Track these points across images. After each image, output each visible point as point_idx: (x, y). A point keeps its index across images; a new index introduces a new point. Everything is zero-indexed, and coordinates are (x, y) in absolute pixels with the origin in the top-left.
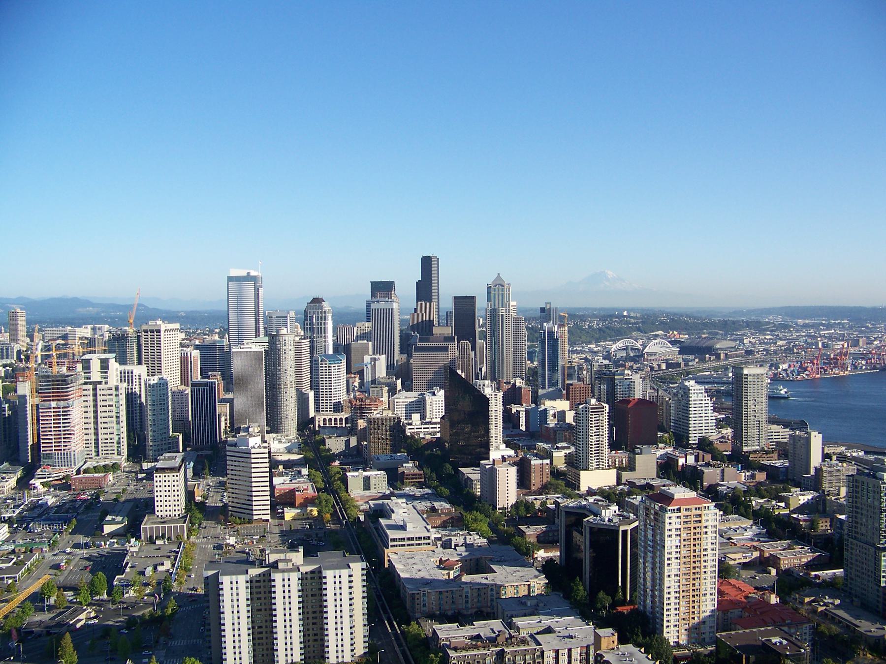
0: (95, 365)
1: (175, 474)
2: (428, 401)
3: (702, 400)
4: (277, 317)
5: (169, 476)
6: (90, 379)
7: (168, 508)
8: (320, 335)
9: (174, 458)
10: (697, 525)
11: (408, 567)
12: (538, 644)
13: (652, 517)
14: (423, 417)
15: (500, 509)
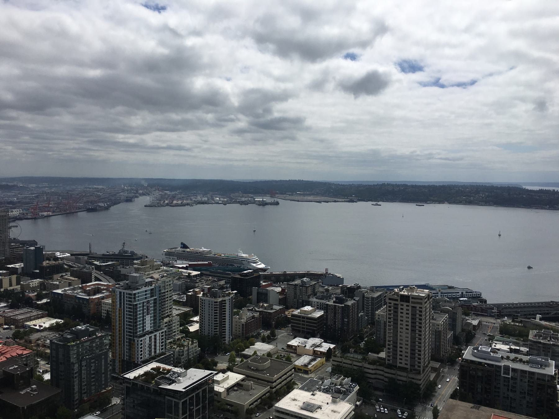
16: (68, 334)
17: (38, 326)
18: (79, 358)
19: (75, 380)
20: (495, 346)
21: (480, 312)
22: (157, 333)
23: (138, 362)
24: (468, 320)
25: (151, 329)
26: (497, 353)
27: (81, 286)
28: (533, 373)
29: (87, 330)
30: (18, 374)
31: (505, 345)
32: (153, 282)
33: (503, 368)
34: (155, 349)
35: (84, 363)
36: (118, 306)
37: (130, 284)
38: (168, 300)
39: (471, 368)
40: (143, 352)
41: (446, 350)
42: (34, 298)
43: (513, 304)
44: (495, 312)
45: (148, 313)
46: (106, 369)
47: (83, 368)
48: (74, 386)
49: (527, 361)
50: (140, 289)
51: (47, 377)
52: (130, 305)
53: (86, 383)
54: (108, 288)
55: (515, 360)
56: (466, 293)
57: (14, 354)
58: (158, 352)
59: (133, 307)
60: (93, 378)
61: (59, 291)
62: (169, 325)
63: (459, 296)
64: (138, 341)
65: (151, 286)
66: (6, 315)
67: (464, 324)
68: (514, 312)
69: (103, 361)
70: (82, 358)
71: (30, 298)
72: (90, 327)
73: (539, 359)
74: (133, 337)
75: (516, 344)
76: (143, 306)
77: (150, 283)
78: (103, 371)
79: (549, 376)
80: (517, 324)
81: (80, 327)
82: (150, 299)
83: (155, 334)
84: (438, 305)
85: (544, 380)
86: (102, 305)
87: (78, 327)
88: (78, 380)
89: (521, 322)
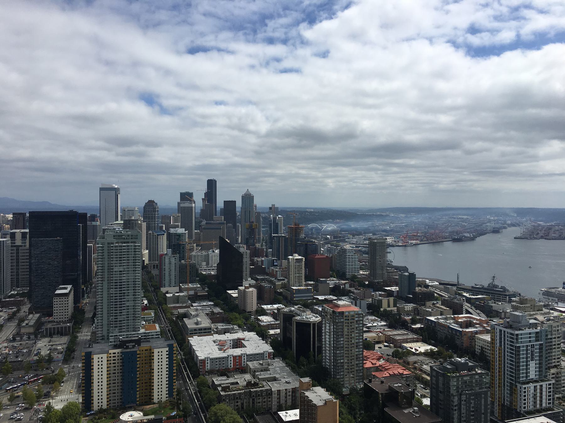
0: (18, 237)
1: (66, 297)
2: (210, 255)
3: (353, 255)
4: (128, 210)
5: (62, 298)
6: (15, 244)
7: (61, 317)
8: (152, 220)
9: (66, 288)
10: (352, 321)
11: (199, 345)
12: (270, 387)
13: (329, 317)
14: (208, 264)
15: (248, 312)
16: (447, 364)
17: (414, 349)
18: (459, 391)
19: (455, 412)
22: (544, 384)
23: (520, 410)
25: (536, 377)
27: (452, 316)
29: (466, 364)
30: (402, 392)
32: (538, 325)
34: (541, 401)
35: (464, 397)
36: (498, 345)
37: (511, 323)
38: (555, 348)
40: (526, 402)
42: (409, 321)
45: (532, 359)
46: (486, 409)
47: (463, 403)
48: (453, 418)
50: (523, 330)
51: (426, 402)
52: (511, 345)
53: (465, 419)
54: (481, 323)
57: (396, 372)
58: (544, 405)
59: (516, 348)
60: (473, 415)
61: (432, 318)
62: (557, 378)
64: (520, 387)
65: (536, 329)
66: (386, 333)
69: (483, 400)
70: (462, 391)
71: (405, 321)
72: (470, 362)
74: (515, 383)
76: (527, 350)
77: (535, 326)
78: (483, 411)
81: (460, 360)
82: (535, 343)
83: (541, 384)
86: (476, 340)
87: (458, 359)
88: (458, 413)
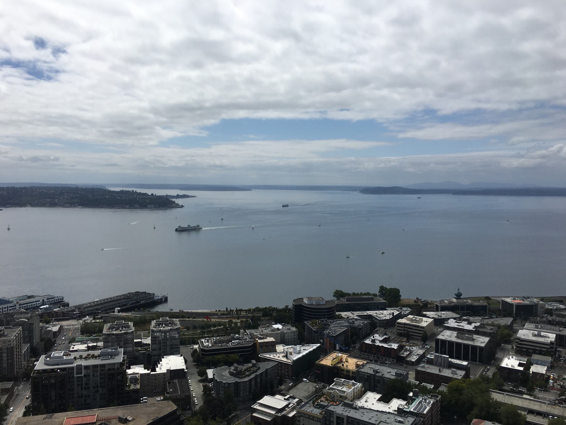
20: (73, 348)
21: (62, 317)
24: (48, 327)
26: (70, 355)
28: (103, 366)
31: (84, 344)
33: (76, 368)
39: (43, 378)
41: (21, 366)
43: (94, 302)
44: (77, 313)
49: (98, 355)
55: (87, 358)
56: (47, 299)
63: (40, 305)
67: (43, 333)
68: (95, 309)
73: (110, 350)
75: (93, 341)
79: (118, 363)
80: (98, 321)
84: (13, 318)
85: (114, 369)
89: (101, 318)
